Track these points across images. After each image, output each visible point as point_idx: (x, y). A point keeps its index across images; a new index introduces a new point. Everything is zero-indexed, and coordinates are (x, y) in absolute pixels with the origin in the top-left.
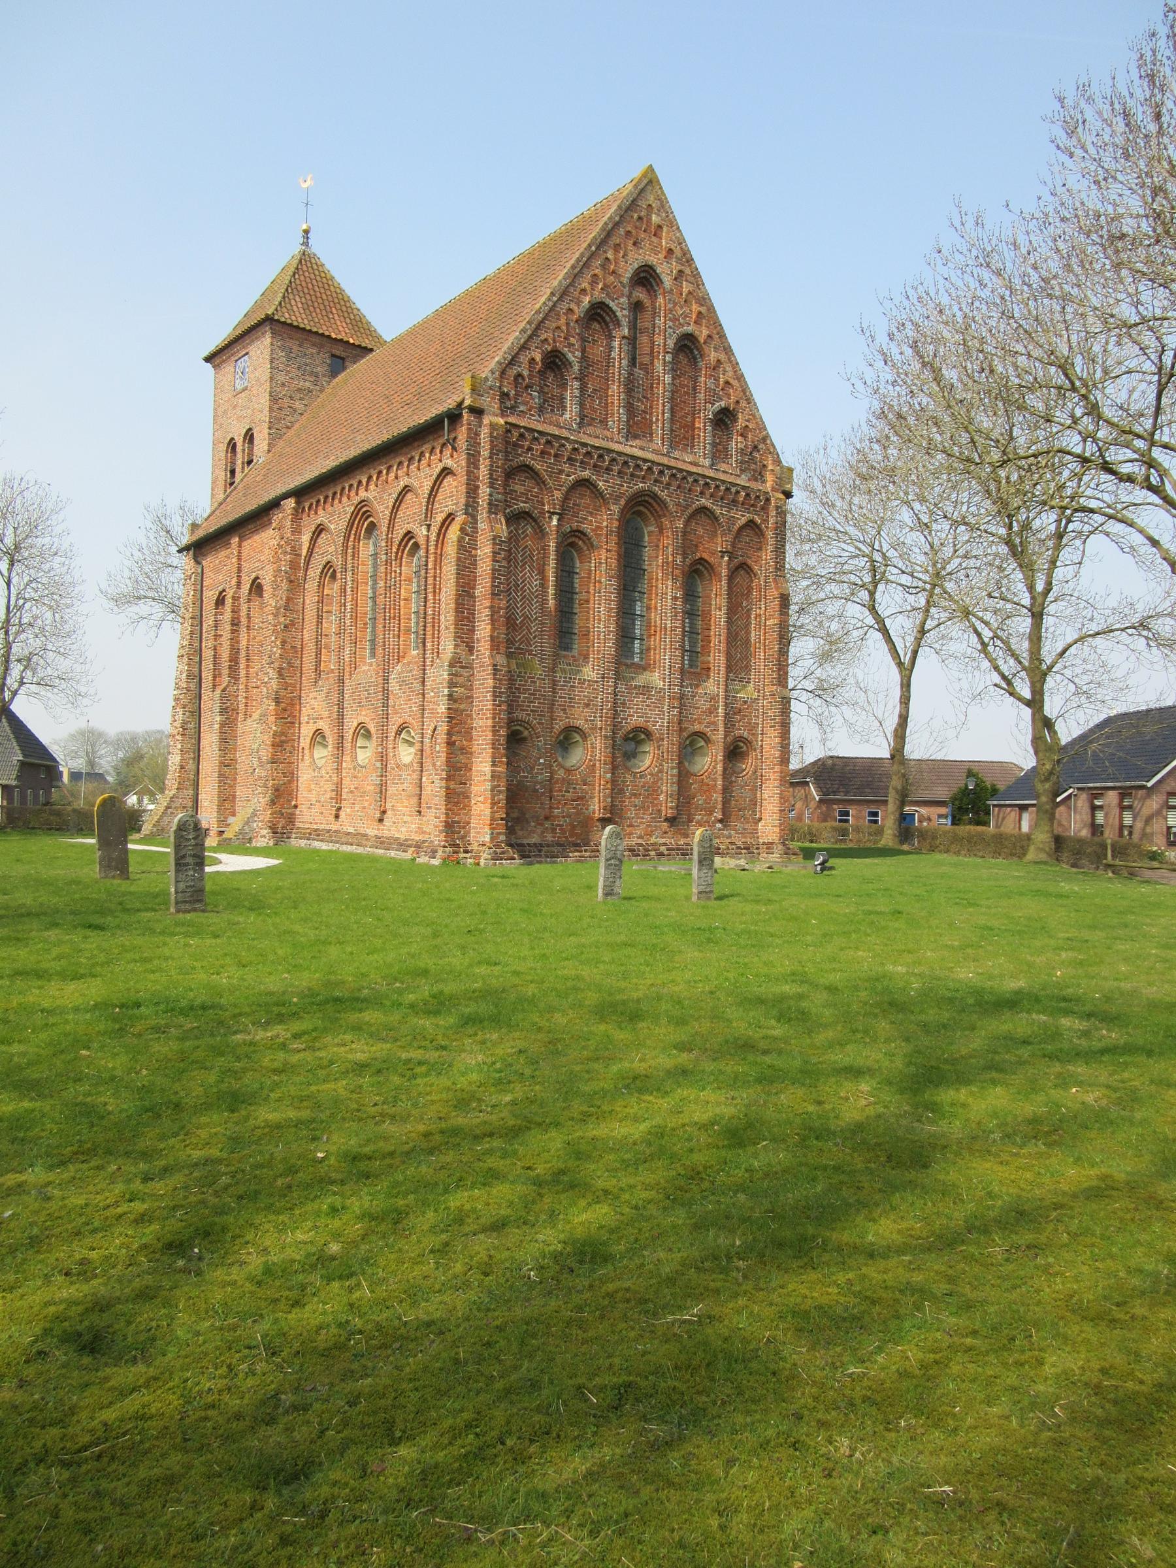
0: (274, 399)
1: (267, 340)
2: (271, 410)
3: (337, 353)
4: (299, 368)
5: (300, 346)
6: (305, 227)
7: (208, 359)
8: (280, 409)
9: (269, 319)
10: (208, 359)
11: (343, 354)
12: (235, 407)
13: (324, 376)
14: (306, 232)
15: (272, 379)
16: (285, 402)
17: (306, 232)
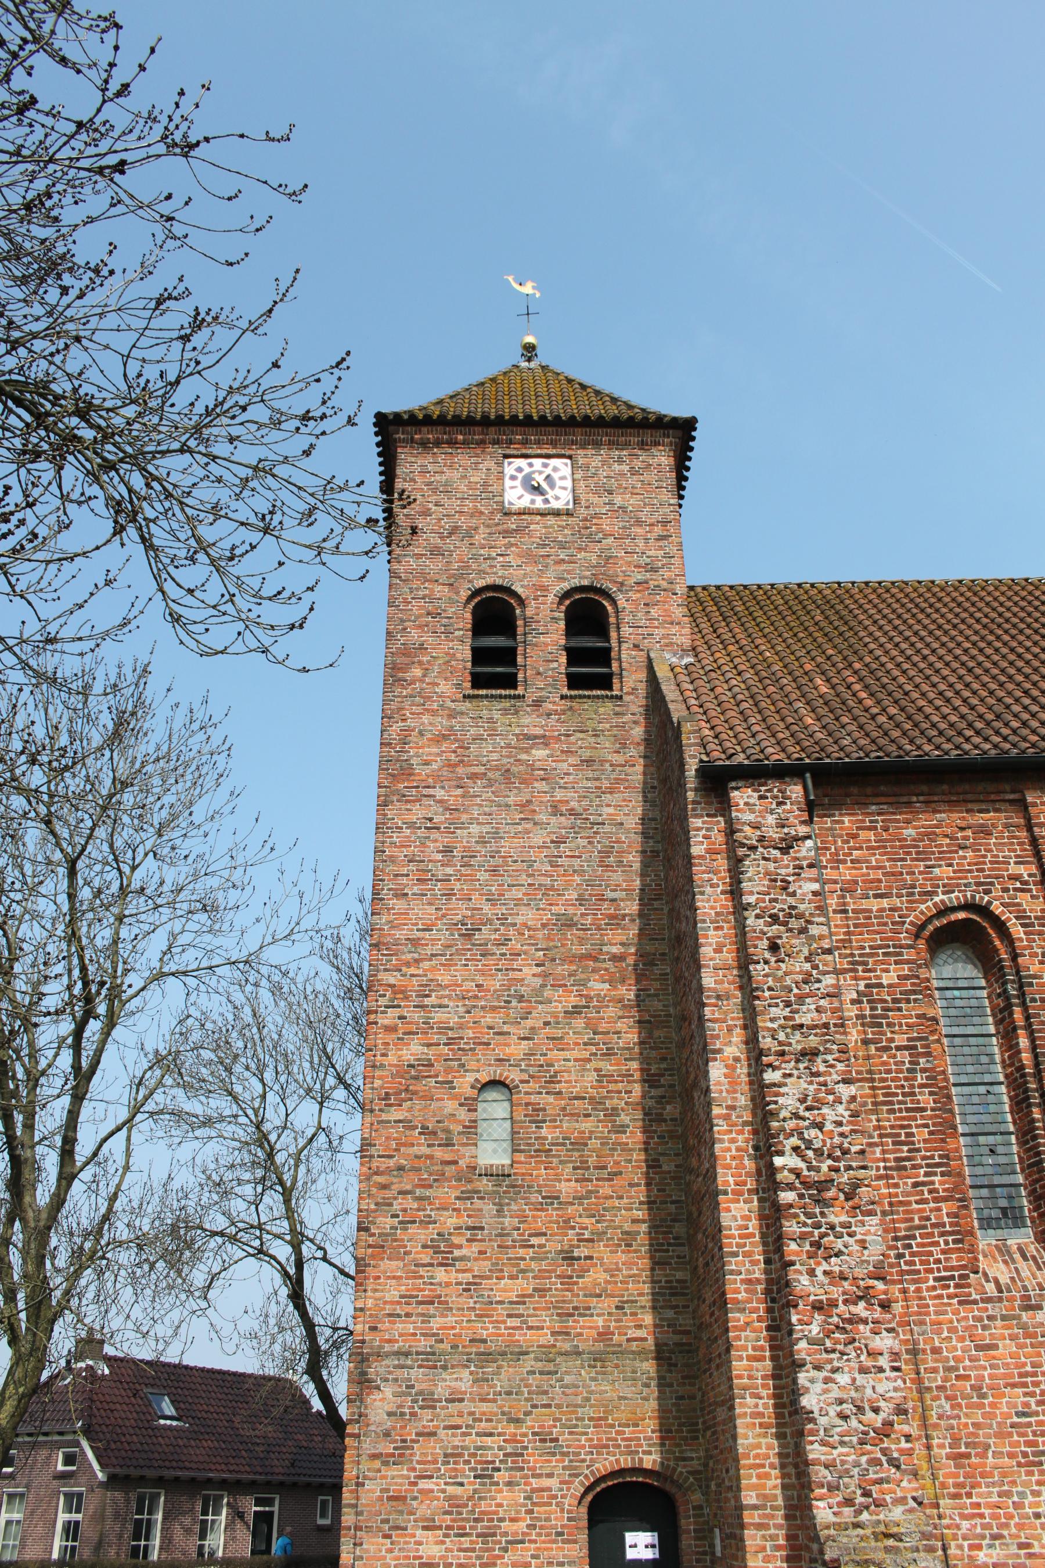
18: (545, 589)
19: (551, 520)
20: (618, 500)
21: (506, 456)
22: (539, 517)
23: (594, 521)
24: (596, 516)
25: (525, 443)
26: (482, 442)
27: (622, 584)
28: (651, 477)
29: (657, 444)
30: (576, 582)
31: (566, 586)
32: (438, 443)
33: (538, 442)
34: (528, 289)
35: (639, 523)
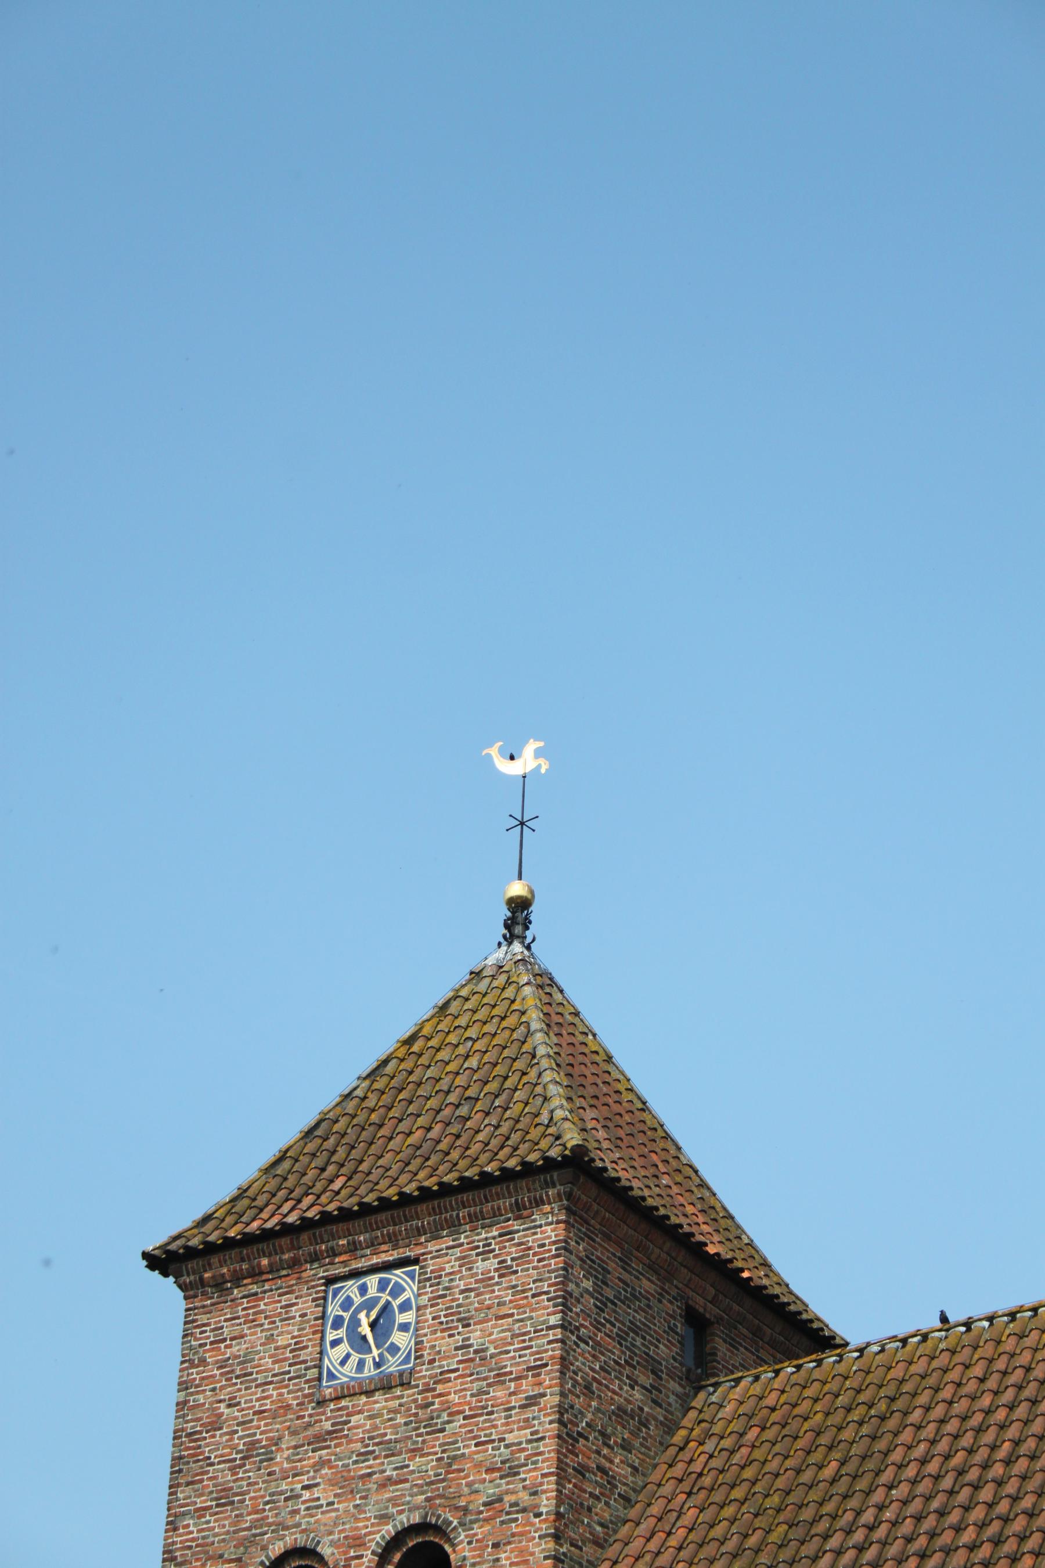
0: (569, 1438)
1: (547, 1229)
2: (561, 1474)
3: (699, 1303)
4: (621, 1338)
5: (625, 1265)
6: (517, 889)
7: (162, 1261)
8: (581, 1471)
9: (577, 1165)
10: (162, 1261)
11: (711, 1311)
12: (319, 1440)
13: (671, 1375)
14: (520, 907)
15: (564, 1362)
16: (587, 1453)
17: (520, 907)
18: (358, 1542)
19: (380, 1402)
20: (476, 1338)
21: (330, 1281)
22: (364, 1399)
23: (440, 1388)
24: (442, 1378)
25: (354, 1248)
26: (295, 1264)
27: (465, 1510)
28: (526, 1276)
29: (539, 1202)
30: (404, 1520)
31: (389, 1530)
32: (237, 1280)
33: (371, 1244)
34: (528, 762)
35: (501, 1378)
